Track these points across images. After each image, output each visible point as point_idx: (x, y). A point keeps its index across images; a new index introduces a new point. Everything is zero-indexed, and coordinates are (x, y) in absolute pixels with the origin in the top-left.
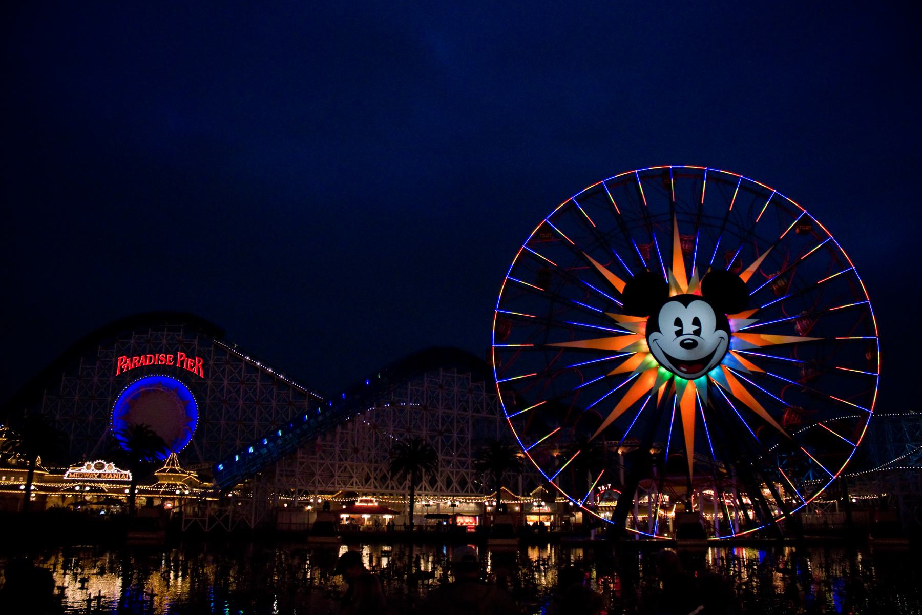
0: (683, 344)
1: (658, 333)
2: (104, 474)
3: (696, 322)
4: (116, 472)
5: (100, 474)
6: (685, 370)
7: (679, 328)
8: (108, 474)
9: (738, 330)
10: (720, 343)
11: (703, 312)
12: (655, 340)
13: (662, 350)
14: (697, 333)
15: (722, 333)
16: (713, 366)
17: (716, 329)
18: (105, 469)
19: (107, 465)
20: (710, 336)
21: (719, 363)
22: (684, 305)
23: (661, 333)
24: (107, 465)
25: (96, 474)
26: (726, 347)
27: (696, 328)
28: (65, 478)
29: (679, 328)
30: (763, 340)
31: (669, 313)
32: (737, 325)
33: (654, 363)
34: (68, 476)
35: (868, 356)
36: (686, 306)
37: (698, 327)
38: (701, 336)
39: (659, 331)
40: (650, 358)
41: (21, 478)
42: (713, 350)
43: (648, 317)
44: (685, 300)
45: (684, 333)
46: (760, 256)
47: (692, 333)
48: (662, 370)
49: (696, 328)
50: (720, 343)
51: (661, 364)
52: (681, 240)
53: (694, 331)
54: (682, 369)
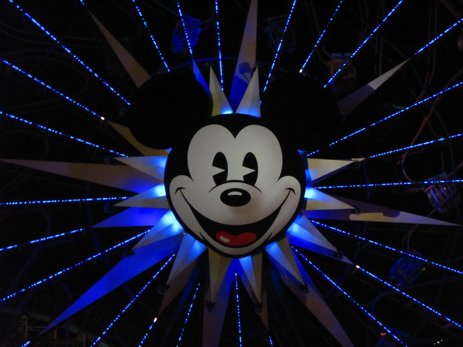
0: (225, 198)
6: (227, 240)
7: (221, 170)
12: (179, 189)
16: (271, 237)
23: (190, 176)
27: (251, 171)
29: (221, 170)
36: (235, 135)
38: (255, 185)
39: (188, 174)
43: (170, 150)
45: (228, 179)
47: (243, 179)
49: (249, 171)
53: (245, 177)
54: (222, 238)
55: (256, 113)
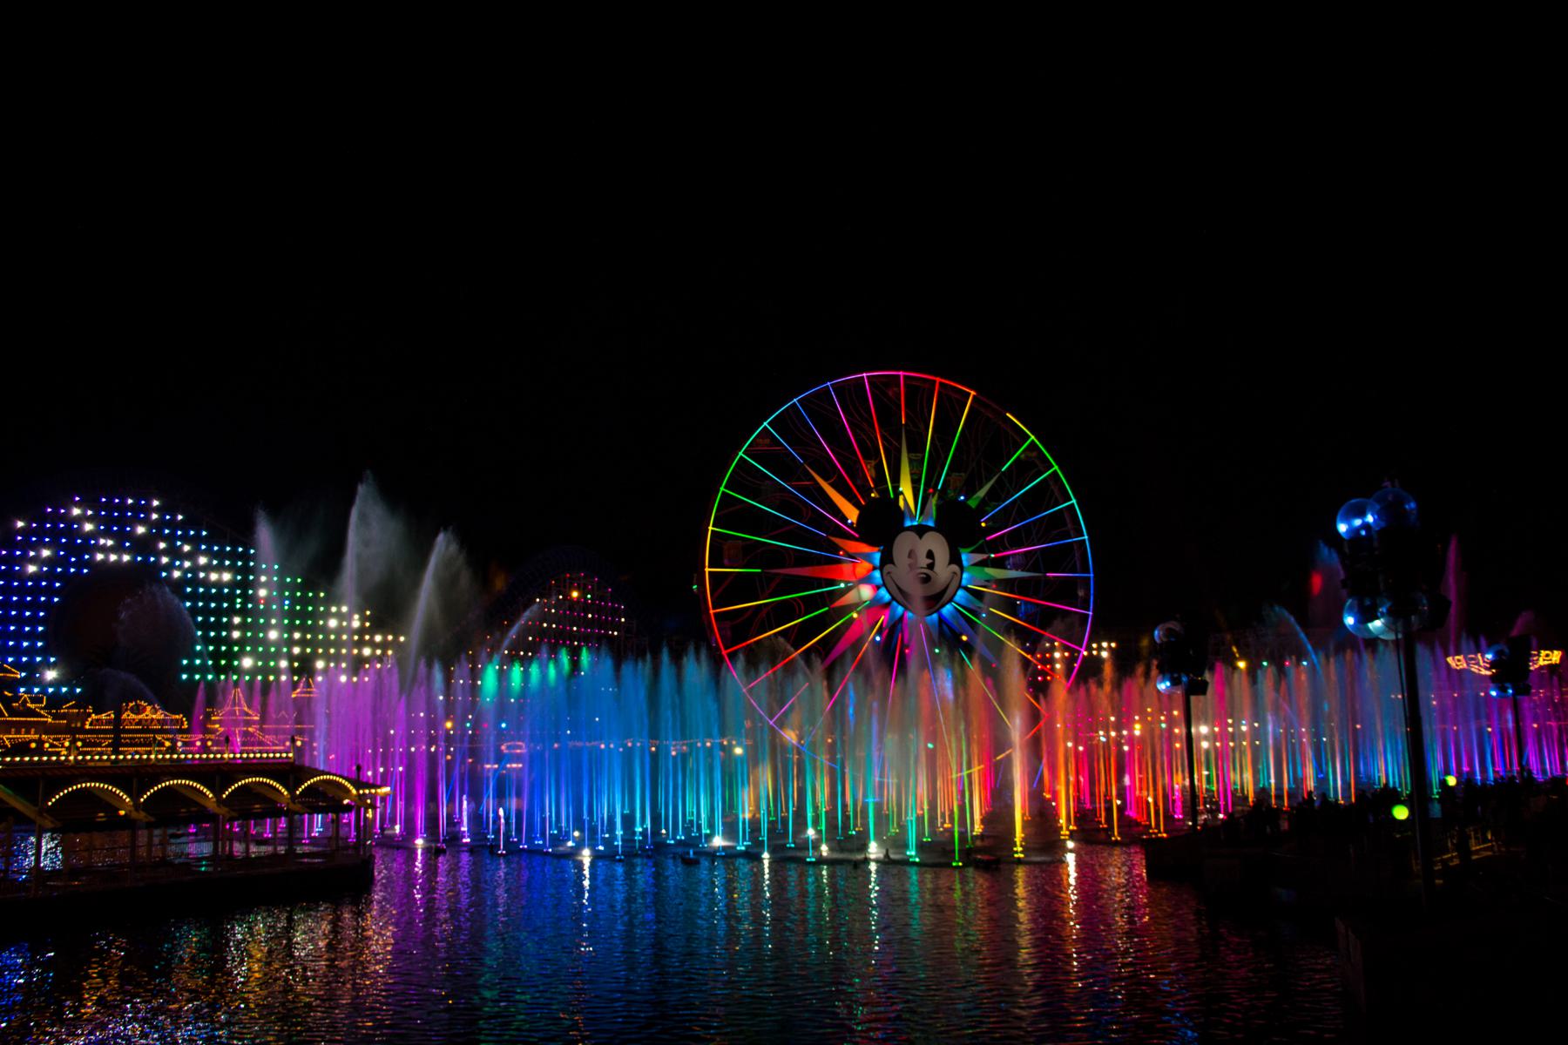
1: (892, 566)
2: (147, 720)
3: (930, 555)
4: (162, 717)
5: (140, 720)
8: (153, 719)
9: (972, 563)
10: (951, 581)
11: (937, 544)
12: (889, 573)
13: (896, 585)
14: (931, 566)
15: (955, 567)
17: (950, 563)
18: (147, 713)
19: (149, 708)
20: (943, 570)
21: (951, 600)
22: (918, 534)
24: (149, 708)
25: (134, 720)
26: (957, 585)
27: (931, 561)
28: (87, 727)
30: (987, 574)
31: (903, 543)
32: (967, 560)
33: (887, 597)
34: (91, 725)
35: (1081, 593)
36: (921, 537)
37: (931, 561)
39: (893, 563)
40: (883, 592)
41: (23, 730)
42: (943, 588)
43: (882, 548)
44: (921, 530)
46: (986, 483)
47: (925, 566)
48: (894, 603)
49: (930, 561)
50: (951, 581)
51: (893, 598)
52: (911, 461)
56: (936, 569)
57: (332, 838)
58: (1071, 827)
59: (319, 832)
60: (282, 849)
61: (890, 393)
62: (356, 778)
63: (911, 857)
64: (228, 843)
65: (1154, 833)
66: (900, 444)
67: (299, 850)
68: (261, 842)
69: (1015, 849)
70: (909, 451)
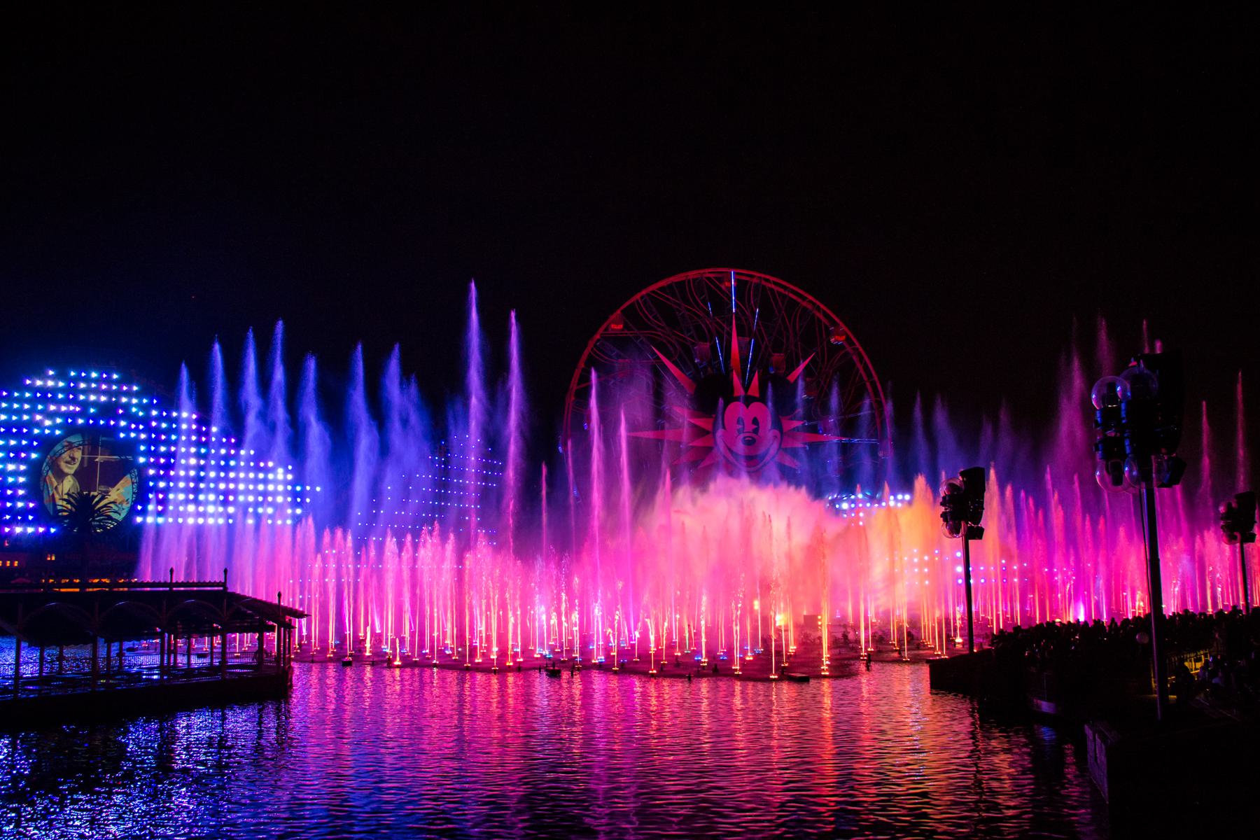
37: (757, 427)
44: (748, 401)
47: (751, 431)
55: (757, 395)
56: (759, 434)
57: (260, 653)
58: (869, 650)
59: (248, 647)
60: (216, 662)
61: (723, 287)
62: (277, 602)
63: (736, 670)
64: (172, 656)
65: (938, 655)
66: (731, 329)
67: (231, 662)
68: (200, 656)
69: (822, 668)
70: (739, 334)
